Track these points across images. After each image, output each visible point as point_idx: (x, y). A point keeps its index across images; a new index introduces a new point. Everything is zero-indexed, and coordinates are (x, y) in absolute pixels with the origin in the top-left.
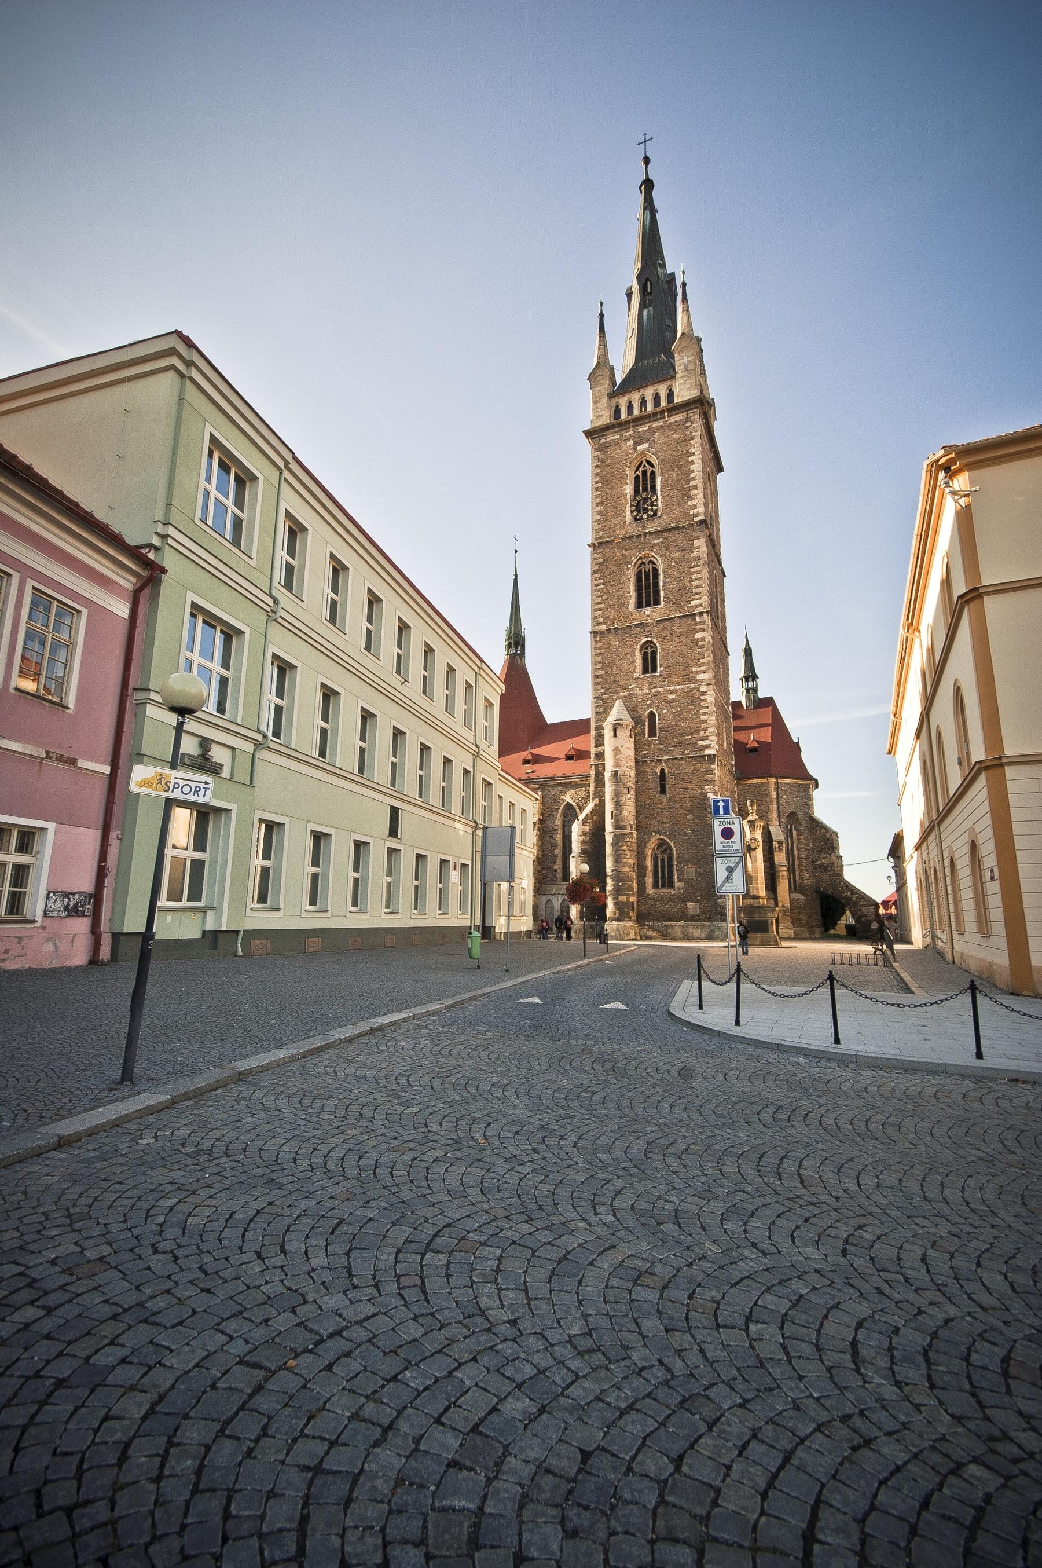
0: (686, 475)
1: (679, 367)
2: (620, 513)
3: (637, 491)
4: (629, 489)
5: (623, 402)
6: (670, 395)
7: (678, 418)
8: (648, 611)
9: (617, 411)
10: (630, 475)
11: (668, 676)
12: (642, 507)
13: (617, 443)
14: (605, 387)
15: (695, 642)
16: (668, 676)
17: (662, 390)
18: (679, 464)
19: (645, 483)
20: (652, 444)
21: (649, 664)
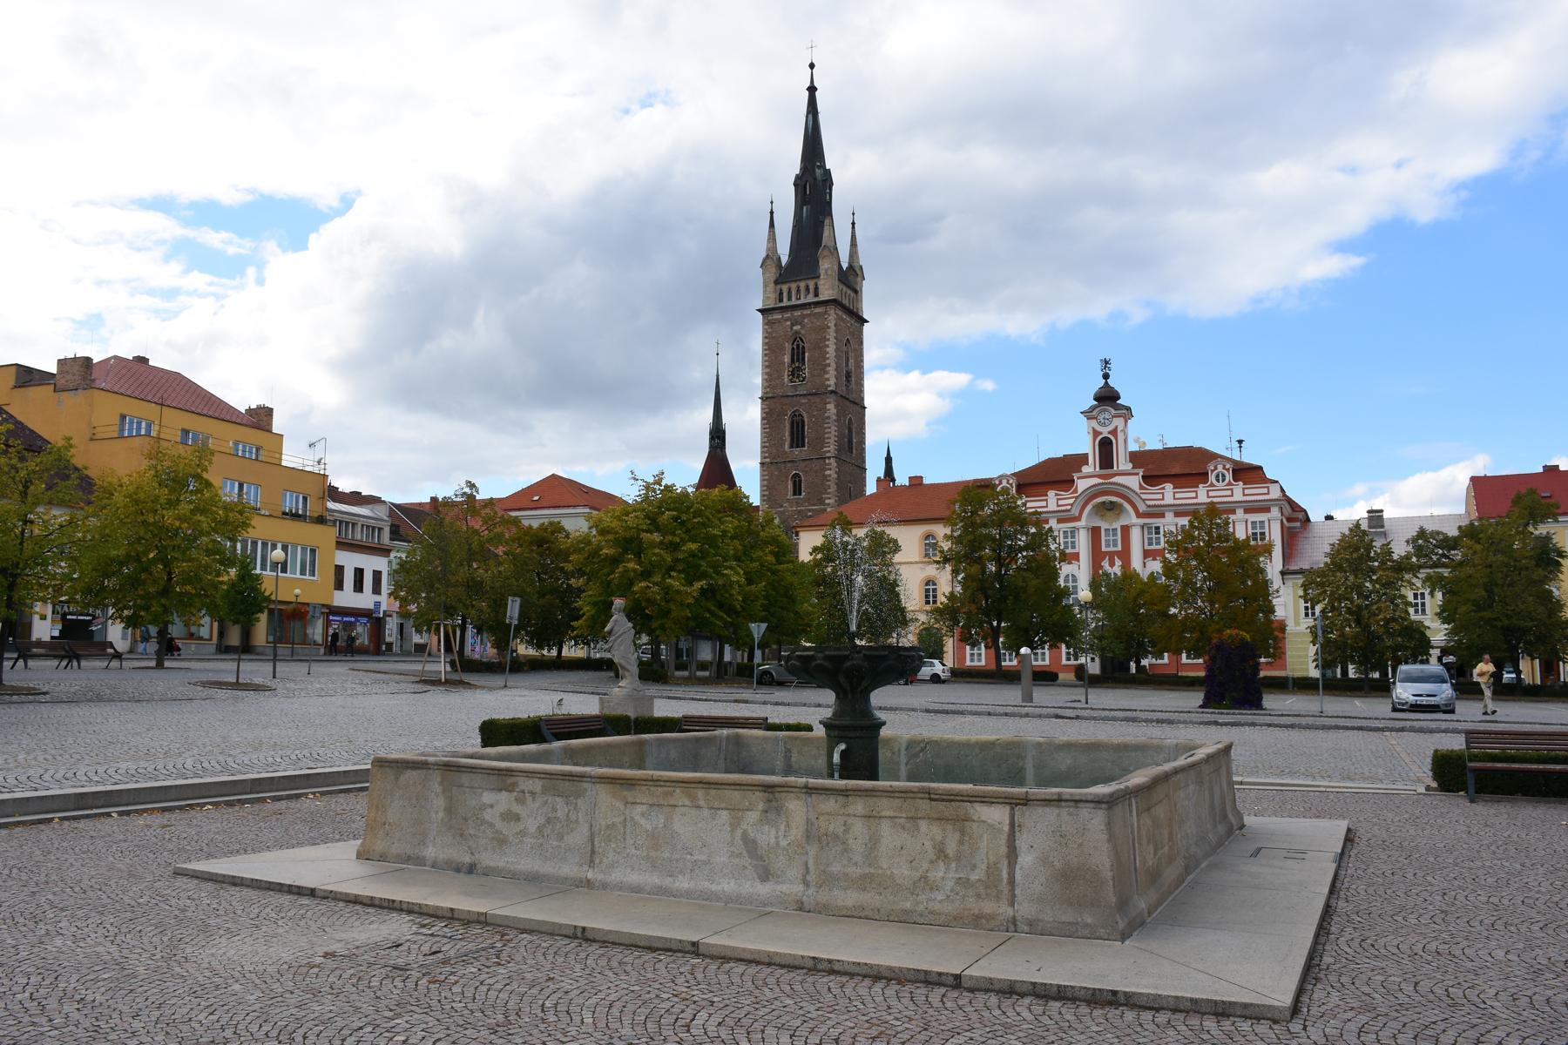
0: (824, 355)
1: (822, 272)
2: (780, 377)
3: (793, 361)
4: (787, 359)
5: (785, 288)
6: (816, 288)
7: (819, 310)
8: (797, 451)
9: (781, 294)
10: (788, 346)
11: (808, 500)
12: (795, 373)
13: (779, 321)
14: (773, 274)
15: (825, 477)
16: (808, 500)
17: (811, 284)
18: (820, 347)
19: (798, 355)
20: (803, 327)
21: (797, 491)
